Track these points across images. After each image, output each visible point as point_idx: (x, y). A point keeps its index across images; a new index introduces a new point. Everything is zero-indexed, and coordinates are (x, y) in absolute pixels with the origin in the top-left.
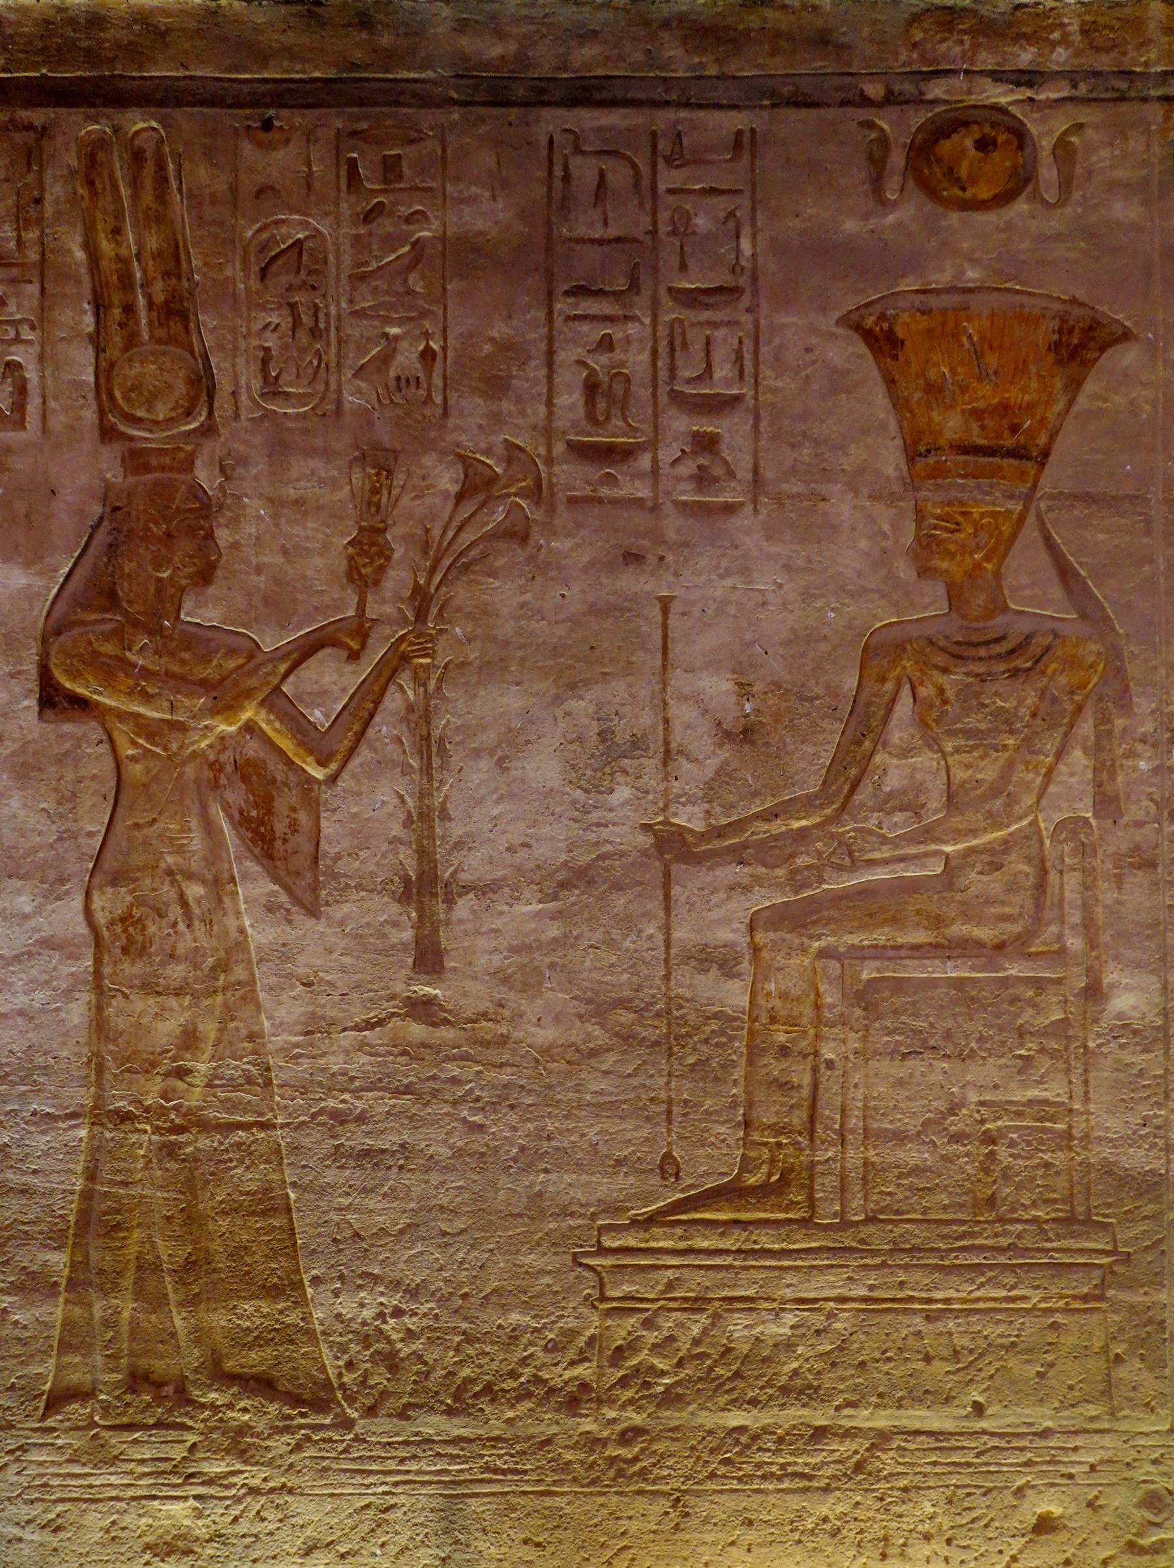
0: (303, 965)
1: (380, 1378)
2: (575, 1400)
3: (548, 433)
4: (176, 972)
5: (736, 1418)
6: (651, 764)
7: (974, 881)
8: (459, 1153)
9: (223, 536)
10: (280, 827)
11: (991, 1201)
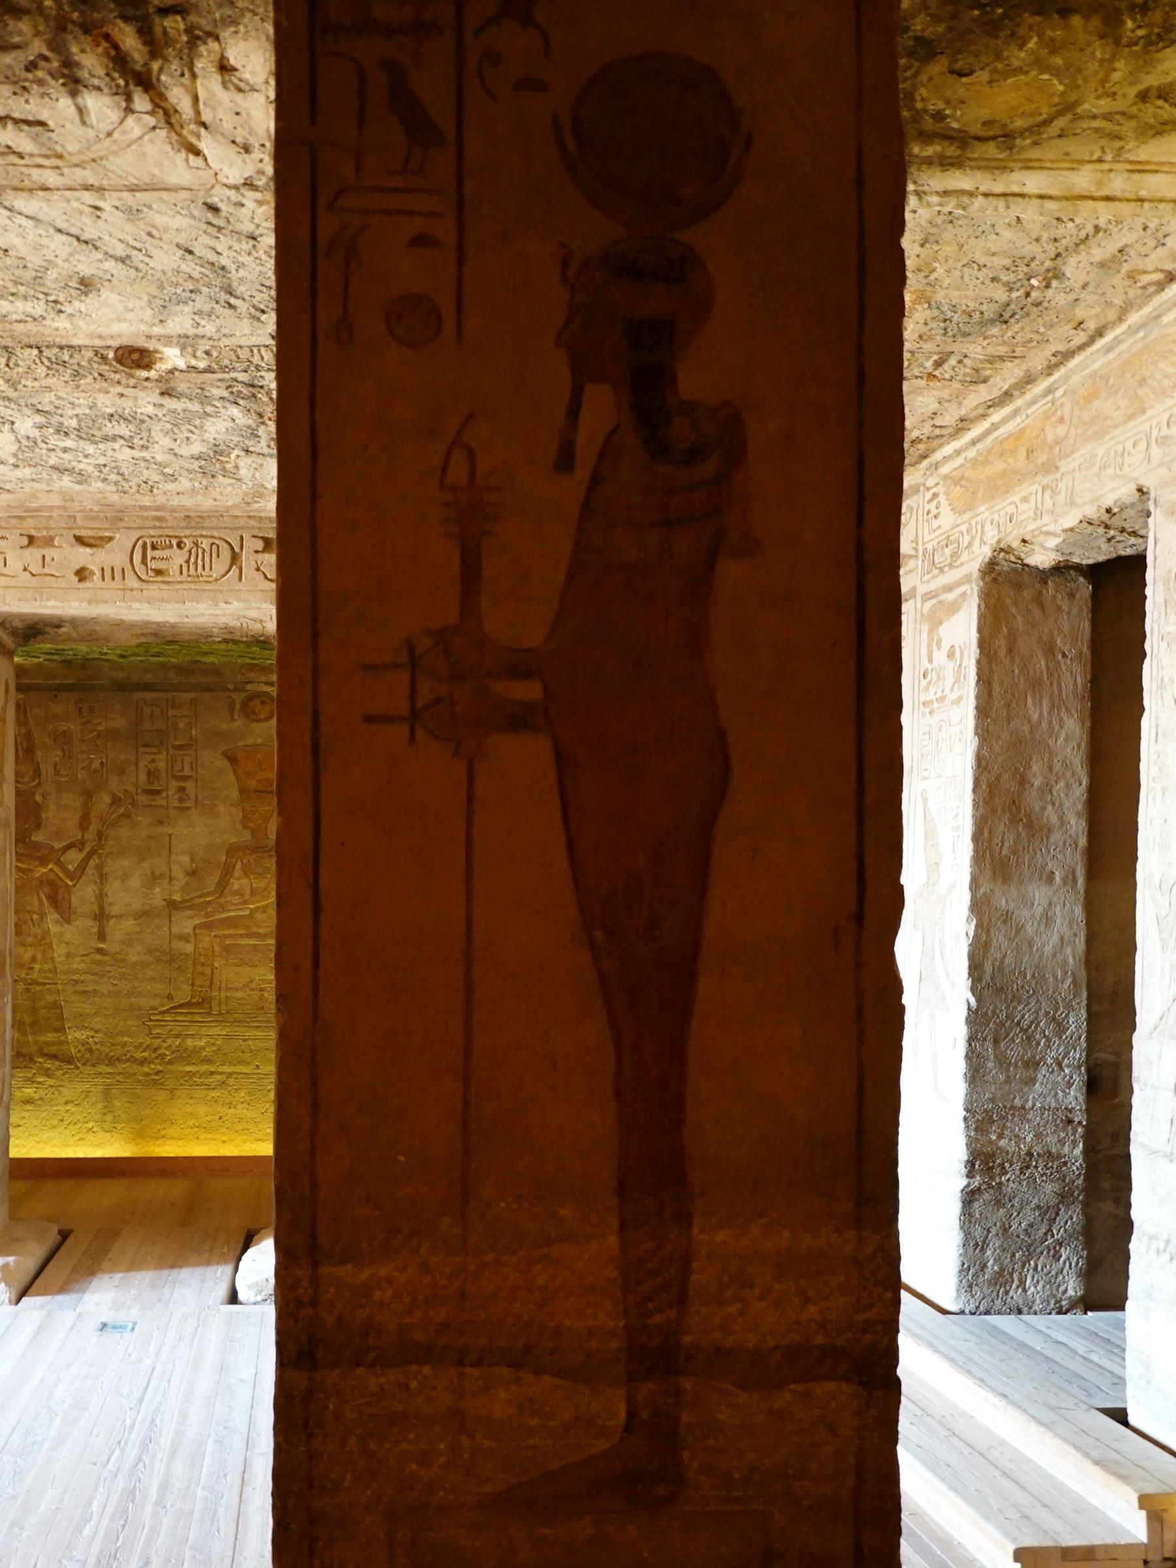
0: (66, 938)
1: (87, 1055)
2: (143, 1062)
3: (136, 786)
4: (30, 940)
5: (188, 1068)
6: (166, 881)
7: (259, 916)
8: (110, 992)
9: (44, 815)
10: (59, 898)
11: (262, 1008)
